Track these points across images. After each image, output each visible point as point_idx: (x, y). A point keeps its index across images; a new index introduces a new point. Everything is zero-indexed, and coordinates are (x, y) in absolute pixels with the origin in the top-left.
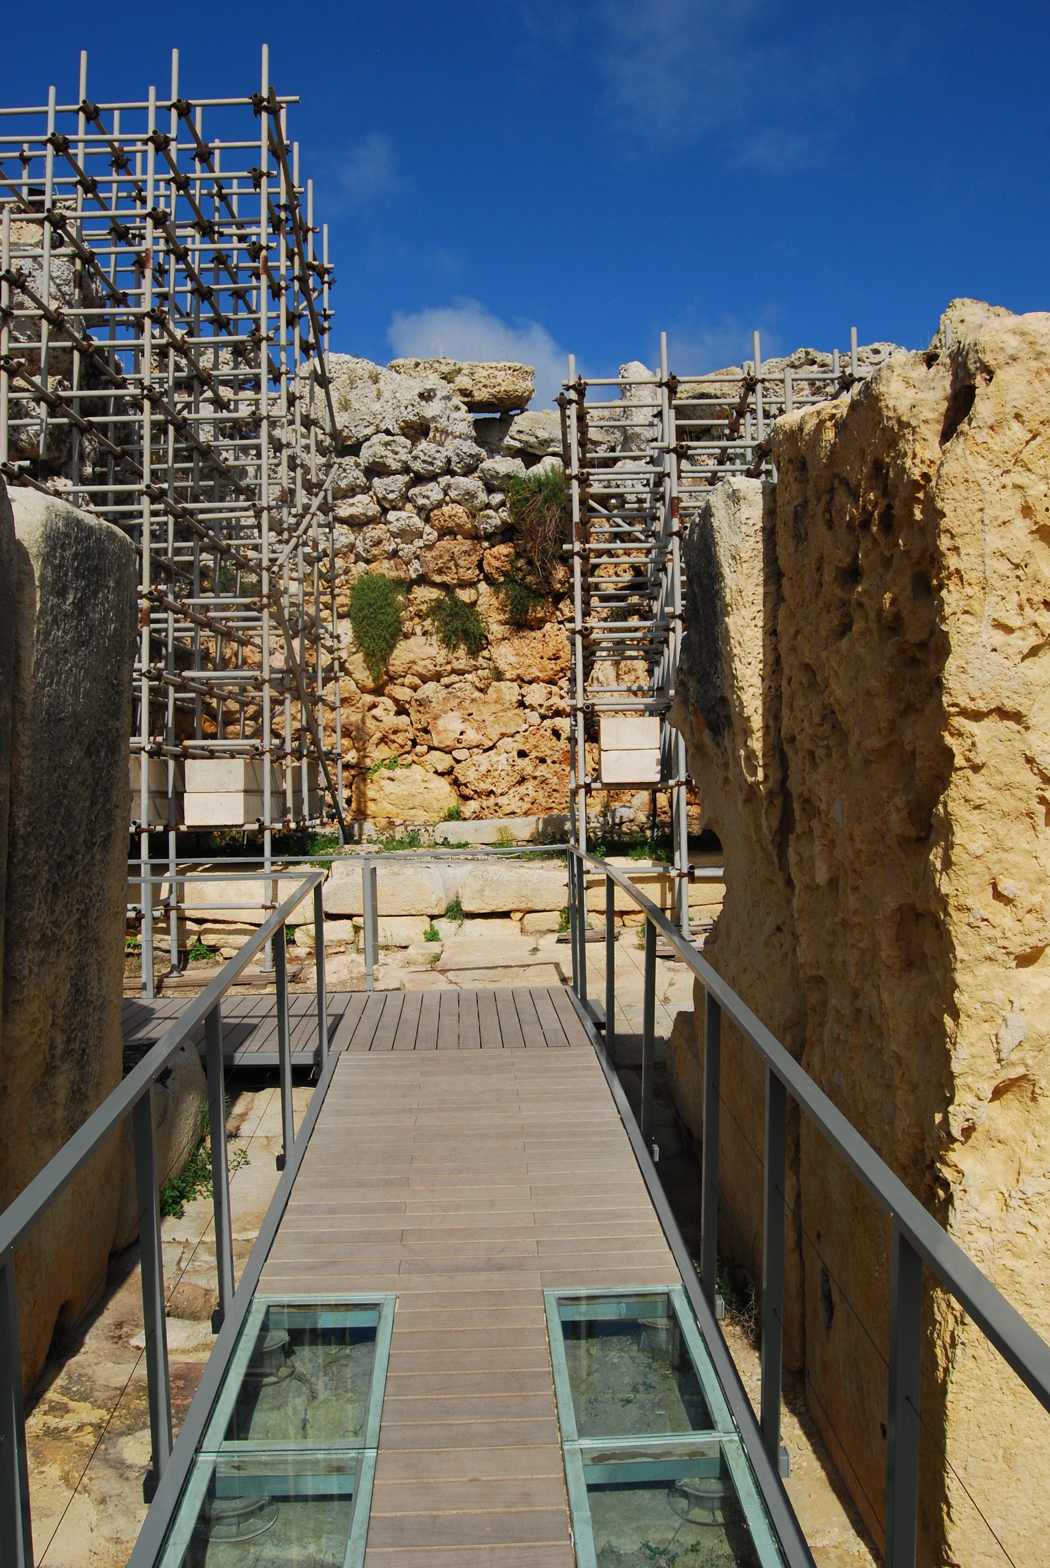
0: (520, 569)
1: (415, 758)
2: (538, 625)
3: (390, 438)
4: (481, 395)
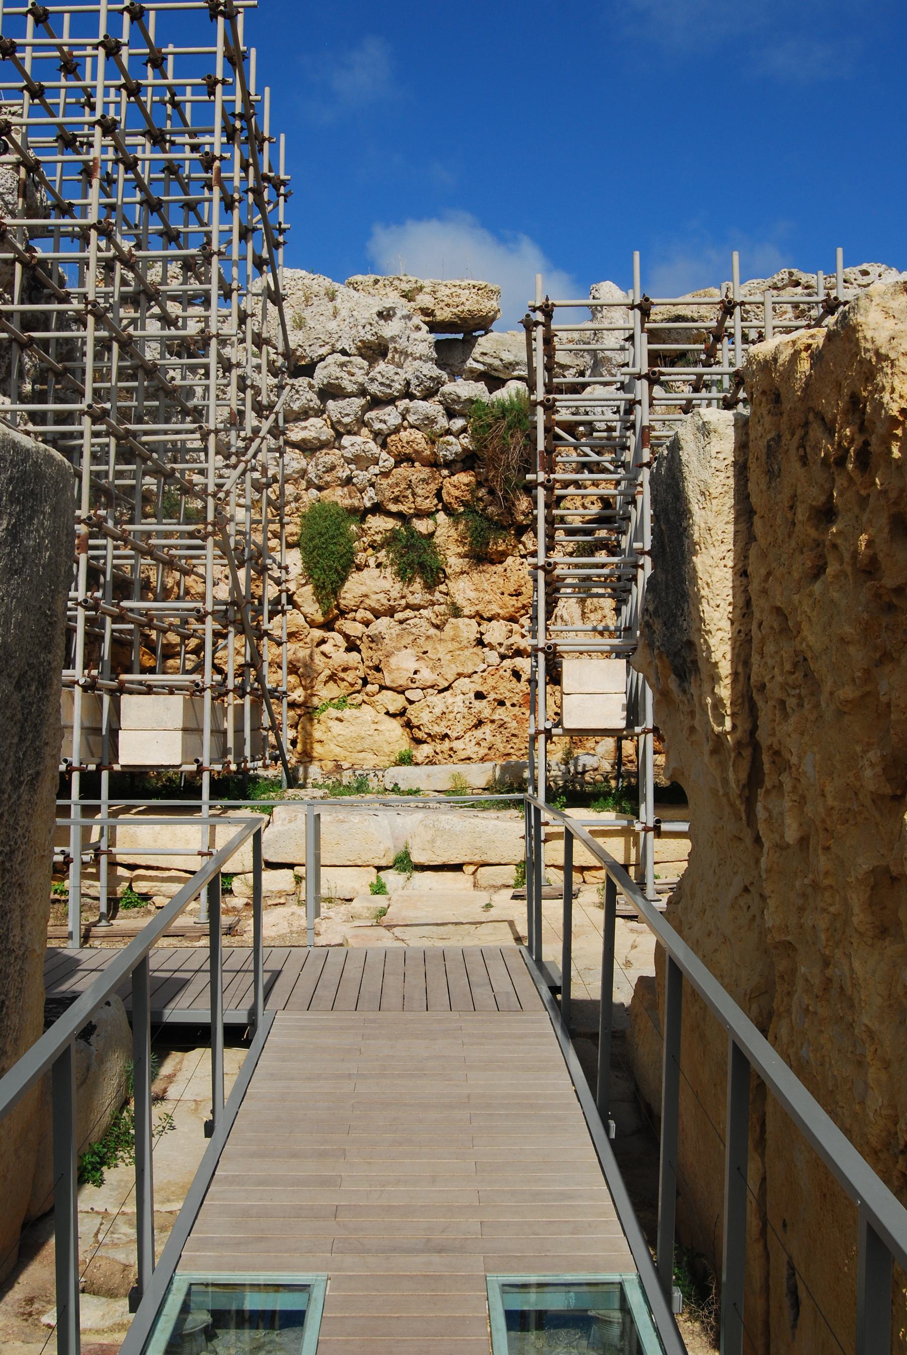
0: (481, 499)
1: (366, 698)
2: (499, 558)
3: (346, 358)
4: (443, 314)
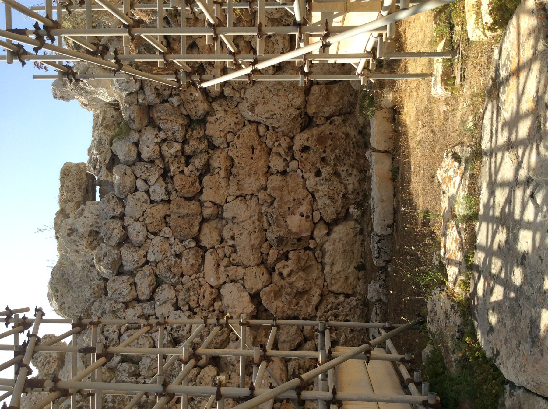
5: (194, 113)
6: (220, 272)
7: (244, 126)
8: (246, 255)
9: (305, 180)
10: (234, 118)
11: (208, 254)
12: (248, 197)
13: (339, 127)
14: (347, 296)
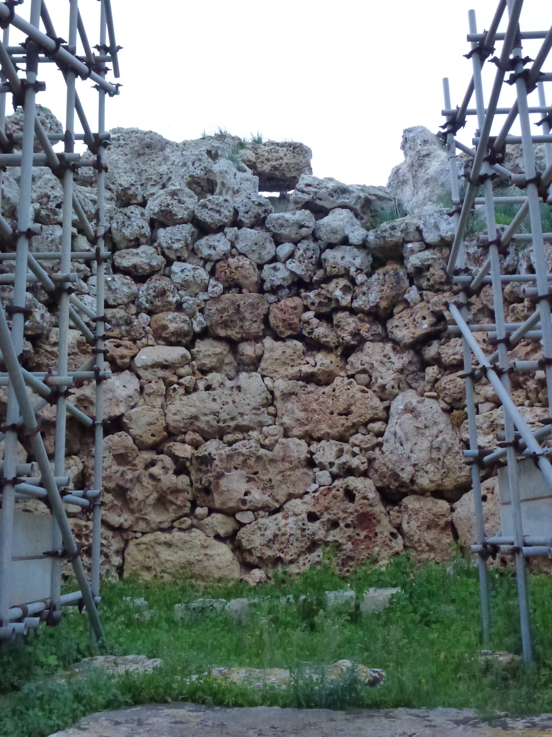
0: (308, 323)
5: (396, 323)
6: (155, 370)
7: (382, 400)
8: (181, 408)
9: (301, 496)
10: (392, 383)
11: (182, 351)
12: (271, 409)
13: (387, 548)
14: (120, 569)
